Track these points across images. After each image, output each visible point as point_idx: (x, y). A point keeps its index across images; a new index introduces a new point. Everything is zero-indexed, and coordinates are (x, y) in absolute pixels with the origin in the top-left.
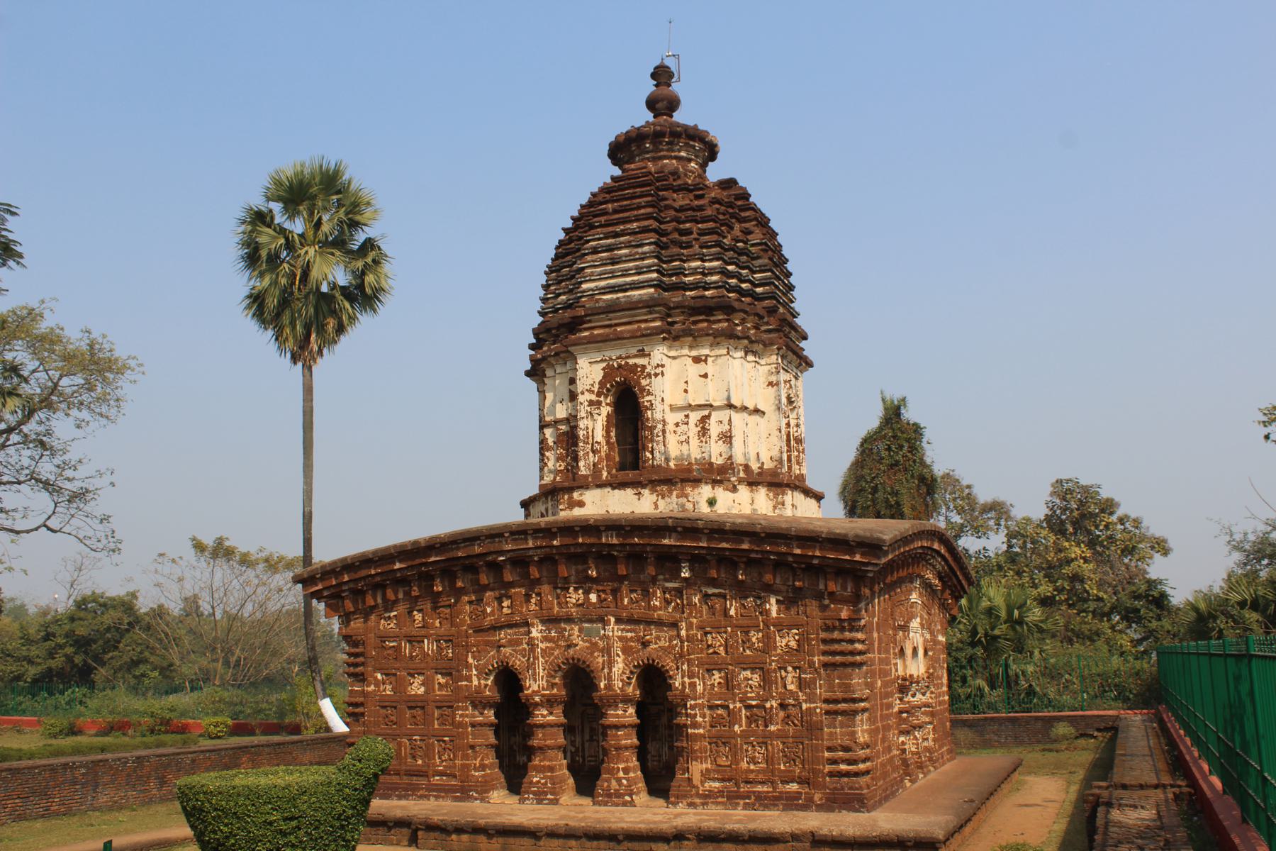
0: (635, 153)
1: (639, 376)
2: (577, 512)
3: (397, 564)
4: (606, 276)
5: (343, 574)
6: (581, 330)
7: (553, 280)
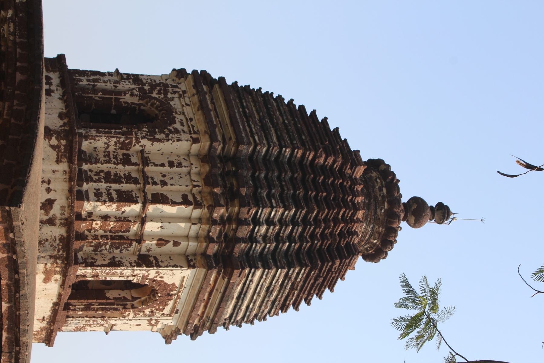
0: (377, 227)
1: (155, 307)
2: (40, 277)
3: (7, 305)
4: (259, 288)
5: (8, 253)
6: (219, 273)
7: (287, 216)
